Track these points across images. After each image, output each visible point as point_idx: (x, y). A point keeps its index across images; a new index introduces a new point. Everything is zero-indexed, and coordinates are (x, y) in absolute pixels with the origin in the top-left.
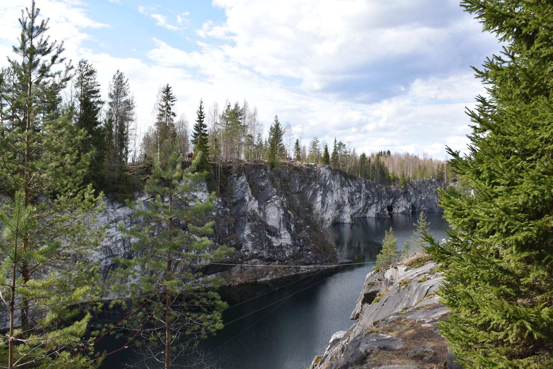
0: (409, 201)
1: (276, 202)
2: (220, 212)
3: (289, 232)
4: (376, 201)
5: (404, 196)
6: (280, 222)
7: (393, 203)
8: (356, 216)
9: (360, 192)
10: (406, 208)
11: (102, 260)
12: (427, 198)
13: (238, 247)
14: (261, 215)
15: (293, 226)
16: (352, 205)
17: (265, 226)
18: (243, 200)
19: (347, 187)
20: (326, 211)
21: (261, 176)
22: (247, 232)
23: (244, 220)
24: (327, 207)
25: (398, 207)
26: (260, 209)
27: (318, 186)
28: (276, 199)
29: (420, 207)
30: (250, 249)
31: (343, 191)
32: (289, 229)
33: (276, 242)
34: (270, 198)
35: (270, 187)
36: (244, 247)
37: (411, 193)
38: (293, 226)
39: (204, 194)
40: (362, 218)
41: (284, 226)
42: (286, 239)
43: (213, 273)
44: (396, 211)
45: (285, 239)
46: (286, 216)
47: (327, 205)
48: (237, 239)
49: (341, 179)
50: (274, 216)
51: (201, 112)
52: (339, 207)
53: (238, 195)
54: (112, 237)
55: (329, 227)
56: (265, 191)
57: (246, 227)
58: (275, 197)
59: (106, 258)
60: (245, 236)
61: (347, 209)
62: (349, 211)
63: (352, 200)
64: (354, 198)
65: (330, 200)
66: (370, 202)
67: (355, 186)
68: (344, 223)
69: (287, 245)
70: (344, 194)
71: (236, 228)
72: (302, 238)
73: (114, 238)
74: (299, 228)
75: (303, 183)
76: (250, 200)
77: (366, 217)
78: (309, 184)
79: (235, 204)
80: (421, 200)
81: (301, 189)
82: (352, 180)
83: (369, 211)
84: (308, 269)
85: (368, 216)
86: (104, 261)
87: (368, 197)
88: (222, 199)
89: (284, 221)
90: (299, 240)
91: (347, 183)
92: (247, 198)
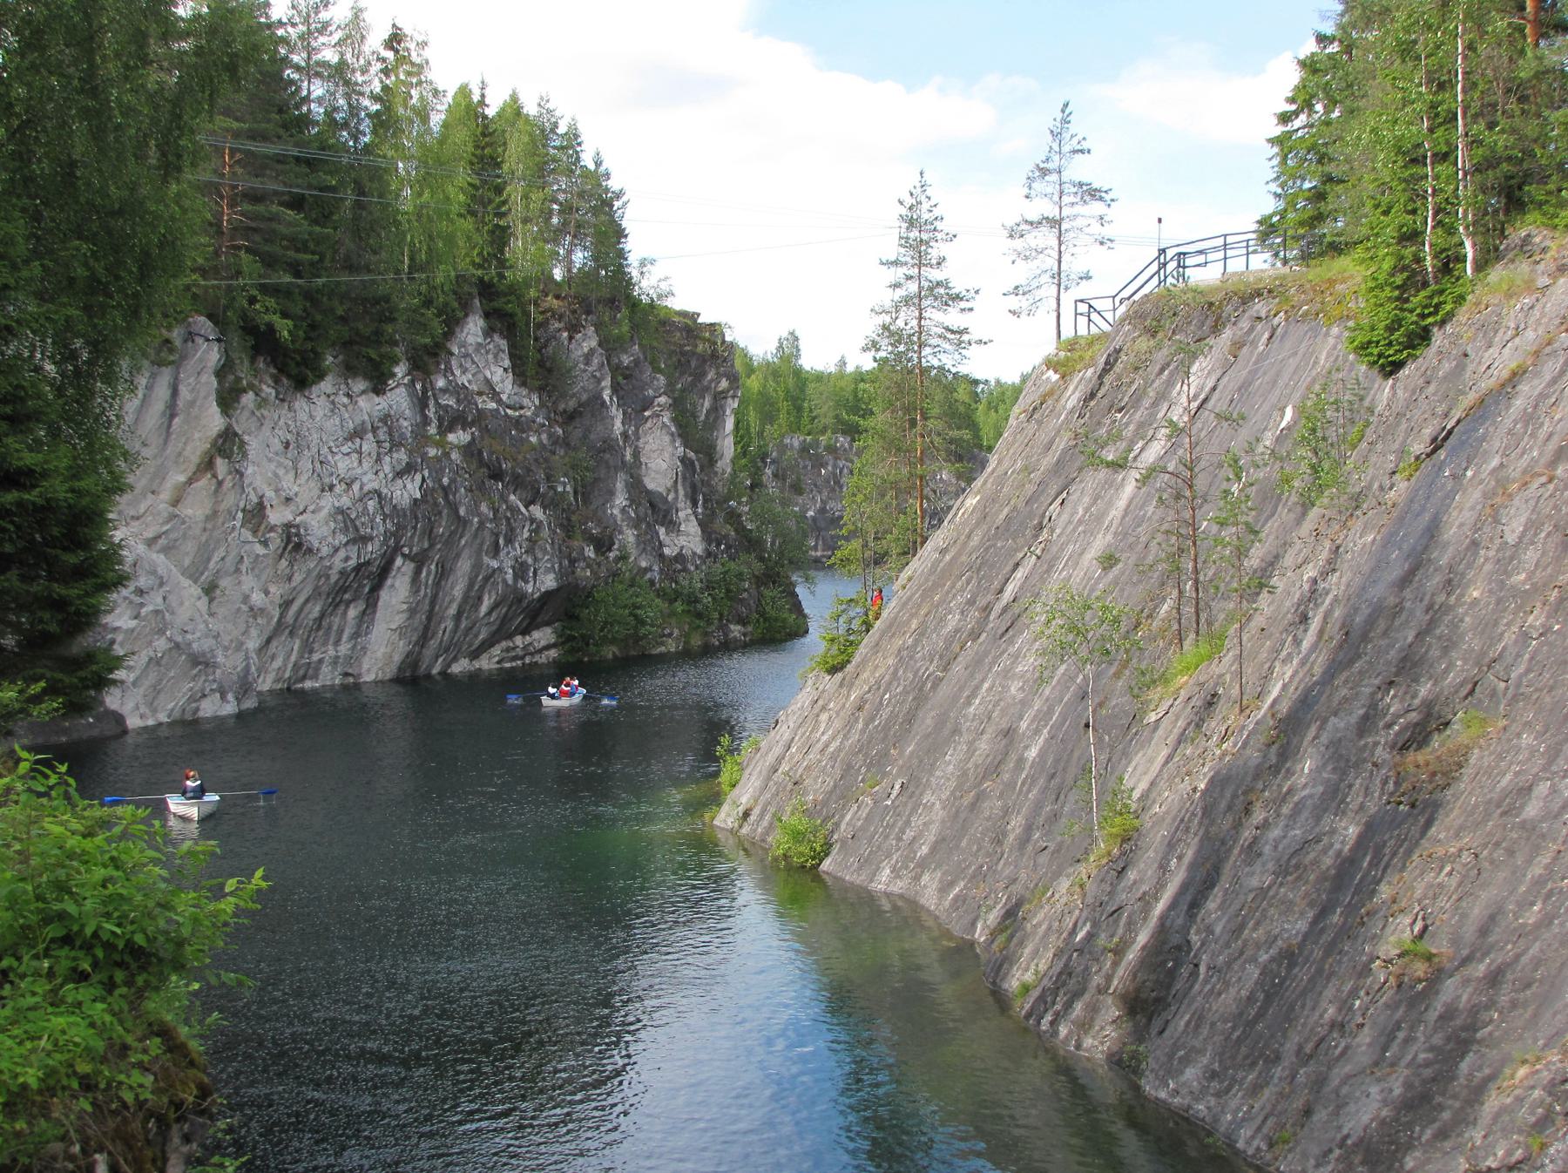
6: (676, 482)
11: (337, 550)
22: (621, 500)
32: (695, 504)
41: (686, 495)
42: (687, 538)
43: (547, 624)
45: (688, 535)
50: (660, 458)
53: (581, 386)
54: (349, 485)
58: (662, 400)
59: (346, 544)
69: (694, 554)
73: (356, 487)
75: (682, 373)
86: (342, 554)
89: (684, 478)
92: (607, 399)
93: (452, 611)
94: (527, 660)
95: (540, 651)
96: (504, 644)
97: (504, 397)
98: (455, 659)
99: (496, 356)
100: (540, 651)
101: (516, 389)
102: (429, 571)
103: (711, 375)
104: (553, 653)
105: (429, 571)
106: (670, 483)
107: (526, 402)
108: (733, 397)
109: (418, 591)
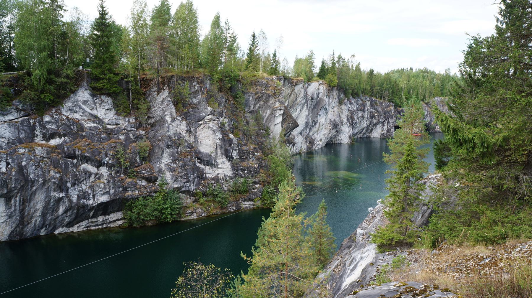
1: (211, 124)
2: (131, 135)
3: (229, 160)
8: (359, 136)
9: (363, 110)
13: (151, 180)
14: (192, 139)
15: (235, 154)
16: (353, 125)
17: (195, 153)
18: (162, 121)
19: (346, 104)
20: (318, 131)
21: (193, 90)
23: (161, 146)
26: (189, 132)
27: (278, 104)
28: (210, 120)
29: (435, 128)
30: (168, 182)
31: (341, 109)
33: (210, 173)
34: (203, 118)
35: (203, 104)
36: (160, 179)
38: (235, 154)
39: (108, 112)
40: (366, 137)
41: (222, 154)
42: (224, 169)
43: (118, 211)
45: (223, 168)
46: (226, 142)
47: (320, 123)
48: (151, 169)
49: (339, 95)
50: (208, 140)
51: (102, 7)
52: (335, 126)
55: (322, 148)
56: (196, 110)
57: (165, 155)
58: (209, 117)
60: (162, 165)
62: (348, 131)
63: (353, 119)
64: (356, 116)
65: (324, 119)
67: (357, 104)
68: (341, 144)
69: (225, 176)
70: (342, 113)
71: (148, 157)
72: (248, 168)
74: (244, 156)
75: (259, 101)
76: (173, 120)
77: (370, 137)
78: (266, 102)
79: (153, 125)
81: (257, 108)
83: (374, 131)
84: (253, 205)
85: (372, 136)
87: (372, 117)
88: (136, 119)
89: (221, 147)
90: (243, 170)
91: (346, 100)
92: (168, 119)
93: (39, 213)
94: (104, 226)
95: (115, 221)
96: (90, 220)
97: (106, 121)
98: (55, 228)
99: (100, 104)
100: (115, 221)
101: (116, 116)
102: (16, 201)
103: (272, 101)
104: (120, 222)
105: (16, 201)
106: (213, 149)
107: (121, 122)
108: (280, 110)
109: (10, 208)
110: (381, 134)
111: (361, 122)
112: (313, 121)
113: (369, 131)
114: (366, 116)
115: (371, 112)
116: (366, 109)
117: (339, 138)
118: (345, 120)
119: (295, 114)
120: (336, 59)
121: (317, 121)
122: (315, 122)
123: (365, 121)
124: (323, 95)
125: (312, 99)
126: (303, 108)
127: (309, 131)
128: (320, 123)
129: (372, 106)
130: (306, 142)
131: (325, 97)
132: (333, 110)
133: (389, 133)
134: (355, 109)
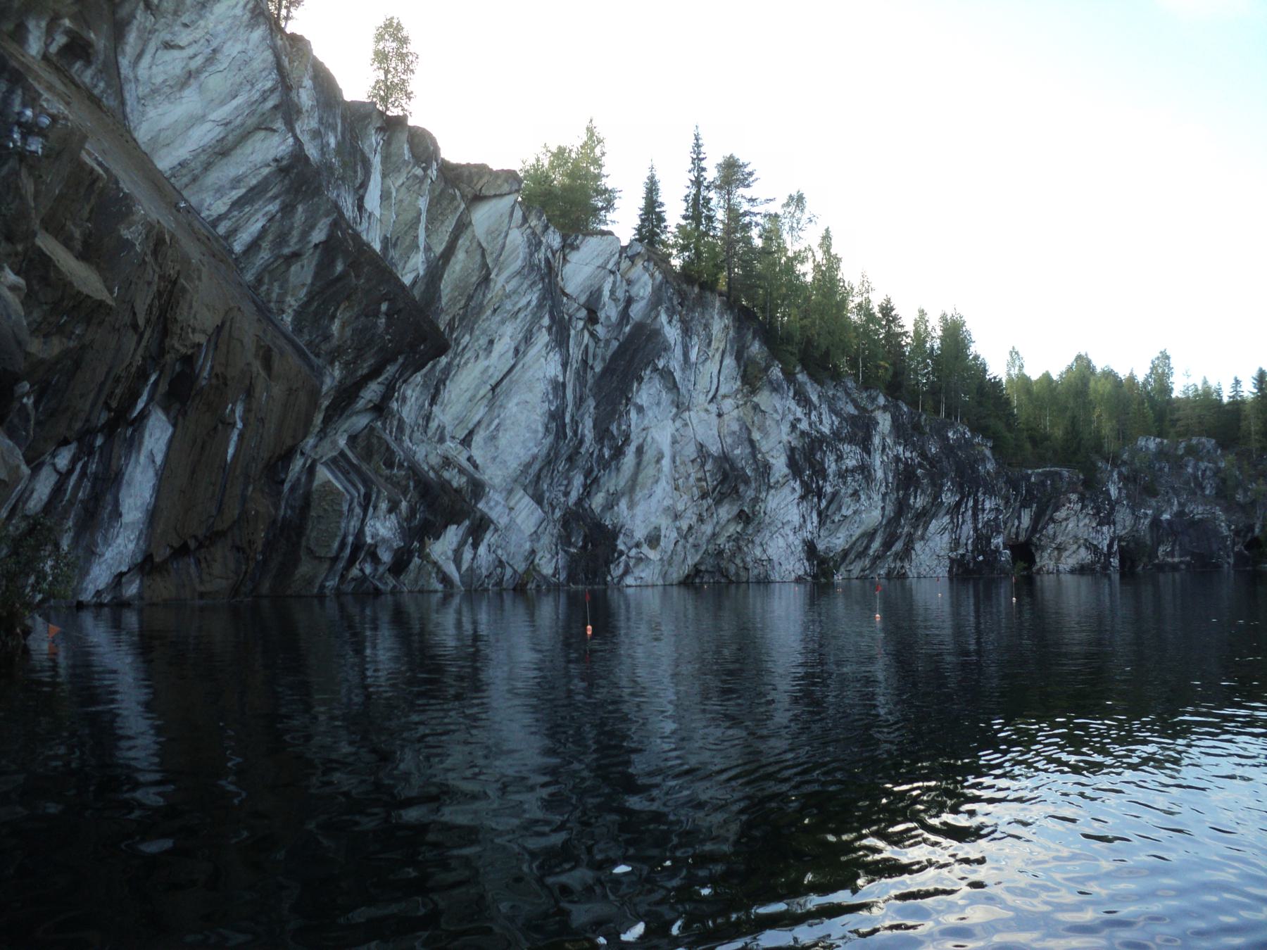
0: (1108, 520)
4: (948, 498)
5: (1082, 499)
7: (1035, 528)
10: (1094, 549)
12: (1181, 514)
24: (638, 464)
25: (1060, 549)
29: (1153, 554)
31: (756, 407)
37: (1114, 492)
44: (1052, 566)
47: (640, 451)
61: (785, 506)
66: (919, 502)
67: (833, 410)
70: (762, 429)
80: (1156, 523)
82: (814, 378)
83: (918, 546)
87: (906, 479)
91: (776, 372)
110: (952, 561)
111: (855, 494)
112: (602, 433)
113: (898, 546)
114: (880, 474)
115: (897, 459)
116: (877, 440)
117: (758, 552)
118: (779, 464)
119: (482, 363)
120: (711, 174)
121: (627, 440)
122: (613, 445)
123: (877, 498)
124: (656, 301)
125: (592, 318)
126: (528, 338)
127: (588, 491)
128: (640, 451)
129: (899, 429)
130: (564, 540)
131: (663, 318)
132: (713, 408)
133: (983, 553)
134: (826, 430)
